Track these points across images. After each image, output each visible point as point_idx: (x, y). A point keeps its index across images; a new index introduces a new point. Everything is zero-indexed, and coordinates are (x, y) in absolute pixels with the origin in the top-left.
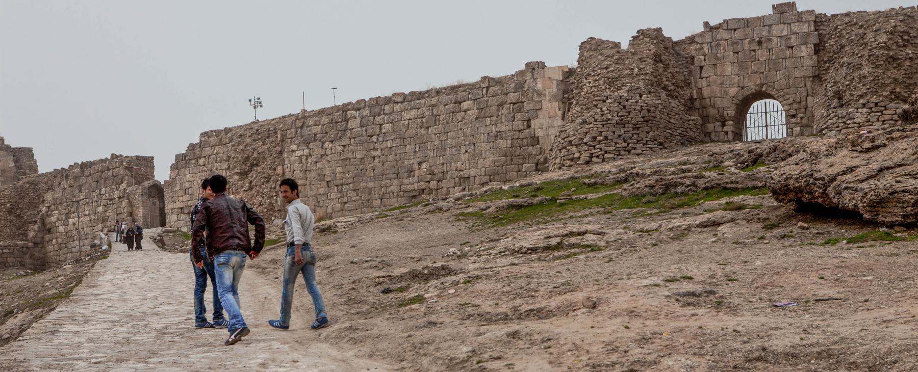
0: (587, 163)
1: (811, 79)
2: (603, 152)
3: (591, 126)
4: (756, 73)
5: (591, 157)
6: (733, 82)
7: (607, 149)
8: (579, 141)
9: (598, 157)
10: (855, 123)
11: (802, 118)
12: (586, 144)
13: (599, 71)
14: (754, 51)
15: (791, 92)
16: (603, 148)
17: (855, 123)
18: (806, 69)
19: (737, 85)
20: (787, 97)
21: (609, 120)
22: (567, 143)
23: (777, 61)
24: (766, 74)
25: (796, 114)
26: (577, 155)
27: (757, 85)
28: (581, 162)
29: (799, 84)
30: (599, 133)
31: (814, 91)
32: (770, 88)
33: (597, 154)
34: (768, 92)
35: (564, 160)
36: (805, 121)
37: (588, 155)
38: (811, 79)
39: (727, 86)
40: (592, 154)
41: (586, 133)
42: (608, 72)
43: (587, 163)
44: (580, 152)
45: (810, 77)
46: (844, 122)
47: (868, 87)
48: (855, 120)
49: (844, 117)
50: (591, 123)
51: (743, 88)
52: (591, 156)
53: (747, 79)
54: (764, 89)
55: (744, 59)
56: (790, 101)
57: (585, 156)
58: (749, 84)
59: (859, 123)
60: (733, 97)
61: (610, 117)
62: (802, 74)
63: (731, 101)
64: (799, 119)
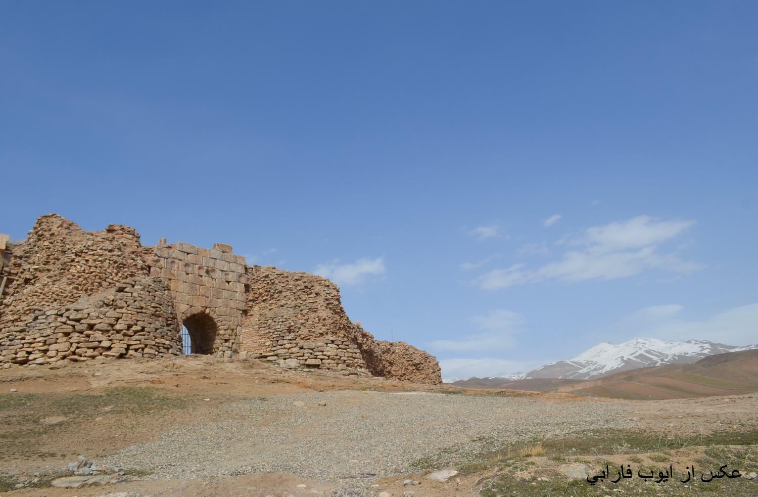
0: (122, 356)
1: (241, 312)
2: (143, 346)
3: (124, 310)
4: (203, 296)
5: (127, 349)
6: (184, 300)
7: (147, 342)
8: (108, 327)
9: (136, 350)
10: (325, 355)
11: (233, 343)
12: (118, 332)
13: (100, 251)
14: (201, 276)
15: (228, 320)
16: (143, 341)
17: (325, 355)
18: (239, 303)
19: (187, 303)
20: (224, 322)
21: (142, 308)
22: (86, 326)
23: (219, 290)
24: (211, 299)
25: (229, 340)
26: (106, 344)
27: (203, 307)
28: (114, 354)
29: (233, 314)
30: (135, 322)
31: (242, 323)
32: (212, 312)
33: (136, 347)
34: (210, 315)
35: (78, 348)
36: (234, 346)
37: (126, 347)
38: (241, 312)
39: (178, 302)
40: (129, 346)
41: (117, 319)
42: (113, 255)
43: (122, 356)
44: (111, 340)
45: (240, 310)
46: (311, 354)
47: (328, 328)
48: (325, 353)
49: (312, 349)
50: (122, 308)
51: (191, 306)
52: (127, 349)
53: (195, 299)
54: (207, 311)
55: (195, 281)
56: (226, 327)
57: (118, 348)
58: (197, 305)
59: (329, 356)
60: (183, 313)
61: (144, 306)
62: (236, 306)
63: (181, 316)
64: (231, 344)
